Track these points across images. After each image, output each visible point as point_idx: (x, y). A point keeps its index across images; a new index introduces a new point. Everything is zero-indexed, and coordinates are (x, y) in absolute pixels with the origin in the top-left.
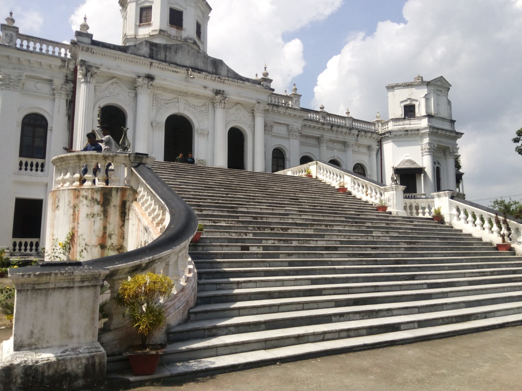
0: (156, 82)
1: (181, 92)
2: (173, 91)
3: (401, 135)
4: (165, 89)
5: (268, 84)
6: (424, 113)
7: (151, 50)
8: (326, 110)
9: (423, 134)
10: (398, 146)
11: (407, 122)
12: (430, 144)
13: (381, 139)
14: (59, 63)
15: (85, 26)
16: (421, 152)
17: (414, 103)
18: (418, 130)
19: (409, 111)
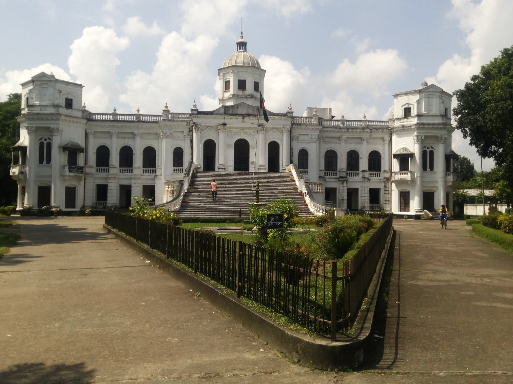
0: (227, 125)
1: (241, 127)
2: (237, 128)
4: (233, 128)
5: (291, 115)
6: (416, 114)
8: (345, 118)
9: (414, 128)
10: (398, 137)
11: (405, 120)
12: (417, 136)
13: (391, 132)
14: (185, 123)
15: (195, 106)
16: (413, 141)
17: (410, 106)
18: (411, 126)
19: (407, 112)
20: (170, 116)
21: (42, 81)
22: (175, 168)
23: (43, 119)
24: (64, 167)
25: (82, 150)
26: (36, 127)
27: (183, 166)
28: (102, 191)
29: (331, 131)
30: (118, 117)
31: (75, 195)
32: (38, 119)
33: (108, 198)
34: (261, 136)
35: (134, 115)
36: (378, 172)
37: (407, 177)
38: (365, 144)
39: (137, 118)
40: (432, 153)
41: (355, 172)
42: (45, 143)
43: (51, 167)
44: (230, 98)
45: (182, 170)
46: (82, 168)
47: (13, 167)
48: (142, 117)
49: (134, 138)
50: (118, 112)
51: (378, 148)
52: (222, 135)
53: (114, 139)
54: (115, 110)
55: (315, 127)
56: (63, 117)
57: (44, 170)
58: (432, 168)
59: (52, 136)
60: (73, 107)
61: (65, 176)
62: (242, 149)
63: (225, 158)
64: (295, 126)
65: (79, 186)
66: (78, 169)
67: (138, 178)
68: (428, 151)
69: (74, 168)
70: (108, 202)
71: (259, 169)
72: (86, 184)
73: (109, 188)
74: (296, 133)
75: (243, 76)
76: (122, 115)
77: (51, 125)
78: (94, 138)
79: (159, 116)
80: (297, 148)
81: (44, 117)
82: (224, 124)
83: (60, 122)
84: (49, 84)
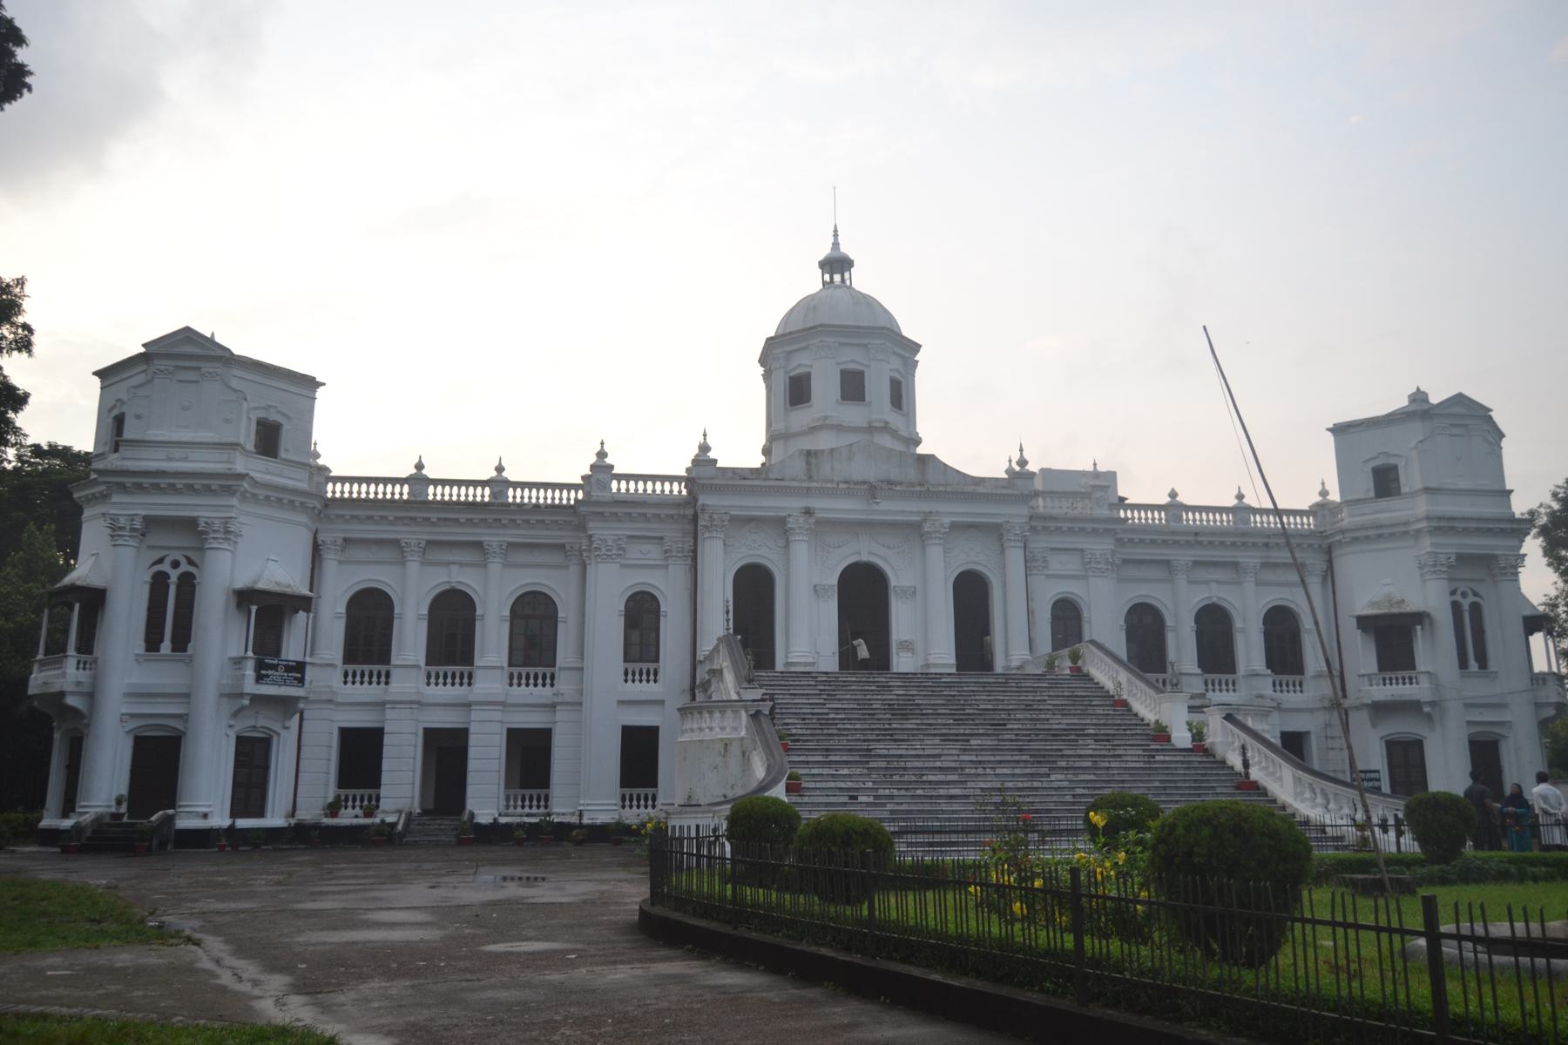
3: (1368, 537)
6: (1419, 486)
7: (808, 463)
8: (1184, 498)
9: (1418, 531)
17: (1393, 461)
18: (1406, 523)
19: (1386, 481)
20: (614, 485)
21: (182, 358)
22: (631, 666)
23: (173, 489)
24: (238, 662)
25: (303, 603)
26: (145, 518)
27: (657, 660)
28: (360, 755)
29: (1141, 541)
30: (431, 489)
31: (266, 768)
32: (157, 488)
33: (385, 777)
34: (935, 552)
35: (483, 484)
36: (1297, 678)
37: (1418, 690)
38: (1249, 585)
39: (492, 495)
40: (1476, 609)
41: (1224, 677)
42: (174, 575)
43: (190, 661)
44: (812, 430)
45: (656, 674)
46: (300, 667)
47: (42, 663)
48: (511, 492)
49: (485, 566)
50: (429, 472)
51: (1295, 599)
52: (801, 551)
53: (413, 567)
54: (420, 466)
55: (1100, 526)
56: (245, 485)
57: (165, 675)
58: (1482, 661)
59: (201, 550)
60: (283, 454)
61: (242, 695)
62: (863, 600)
63: (809, 633)
64: (1039, 524)
65: (283, 733)
66: (288, 669)
67: (492, 700)
68: (1466, 604)
69: (274, 667)
70: (384, 791)
71: (928, 665)
72: (307, 727)
73: (387, 740)
74: (1040, 543)
75: (852, 358)
76: (444, 482)
77: (202, 508)
78: (340, 562)
79: (569, 487)
80: (1049, 592)
81: (179, 483)
82: (808, 512)
83: (234, 501)
84: (207, 367)
